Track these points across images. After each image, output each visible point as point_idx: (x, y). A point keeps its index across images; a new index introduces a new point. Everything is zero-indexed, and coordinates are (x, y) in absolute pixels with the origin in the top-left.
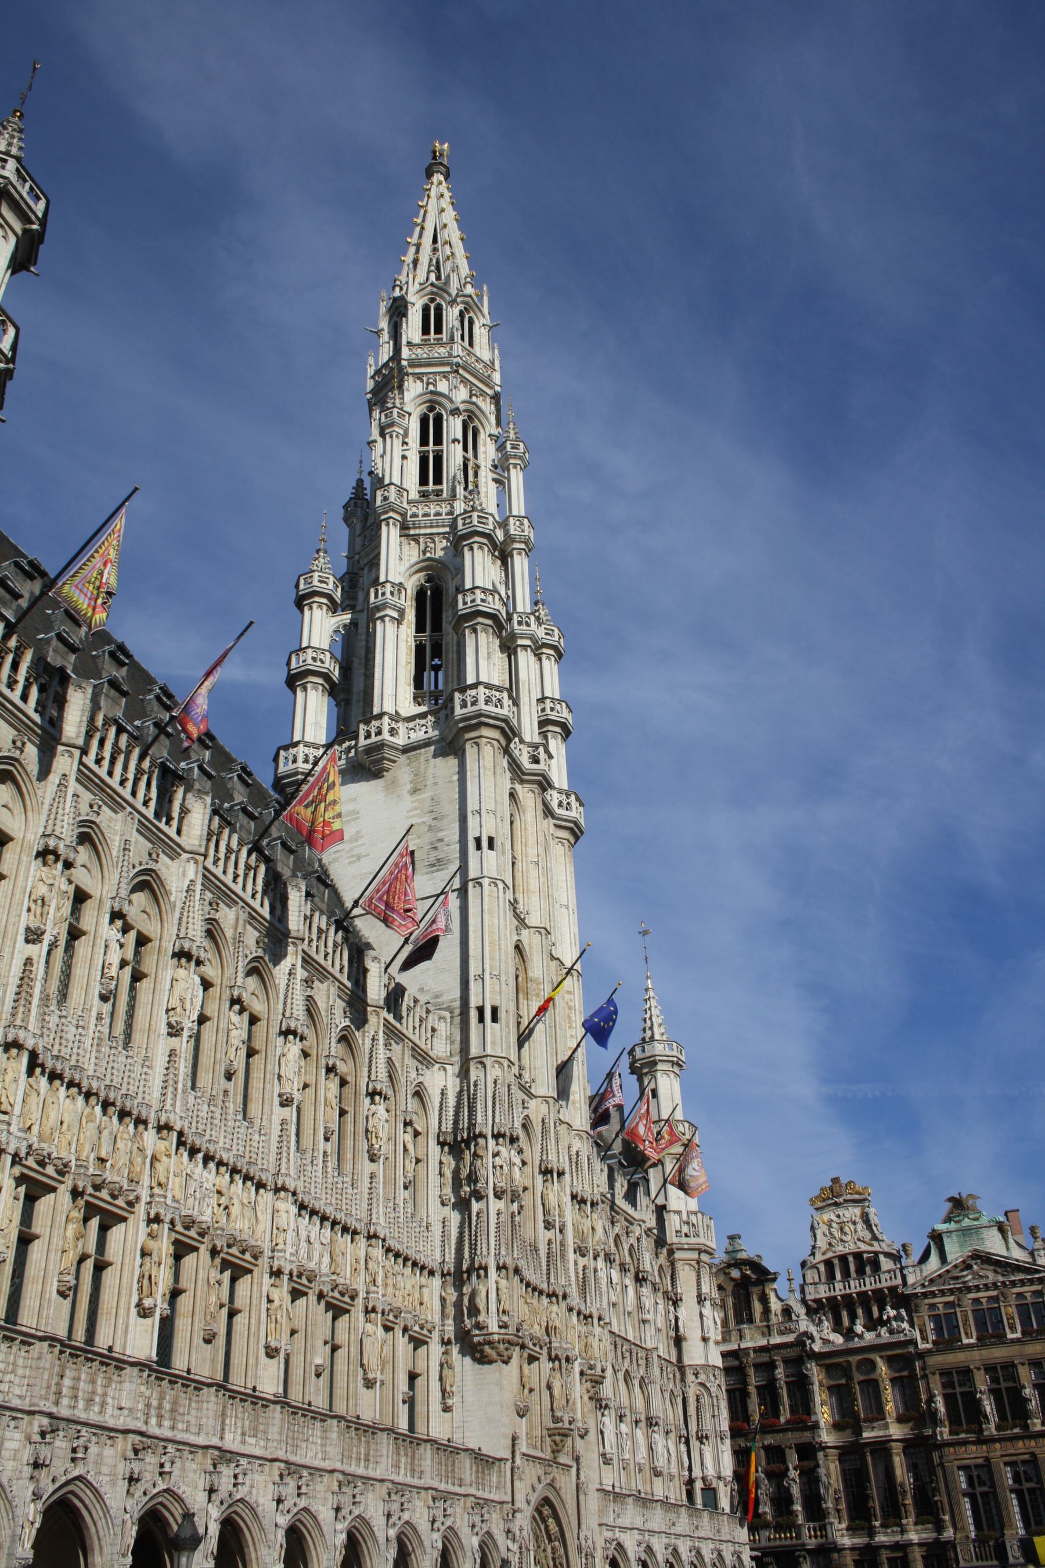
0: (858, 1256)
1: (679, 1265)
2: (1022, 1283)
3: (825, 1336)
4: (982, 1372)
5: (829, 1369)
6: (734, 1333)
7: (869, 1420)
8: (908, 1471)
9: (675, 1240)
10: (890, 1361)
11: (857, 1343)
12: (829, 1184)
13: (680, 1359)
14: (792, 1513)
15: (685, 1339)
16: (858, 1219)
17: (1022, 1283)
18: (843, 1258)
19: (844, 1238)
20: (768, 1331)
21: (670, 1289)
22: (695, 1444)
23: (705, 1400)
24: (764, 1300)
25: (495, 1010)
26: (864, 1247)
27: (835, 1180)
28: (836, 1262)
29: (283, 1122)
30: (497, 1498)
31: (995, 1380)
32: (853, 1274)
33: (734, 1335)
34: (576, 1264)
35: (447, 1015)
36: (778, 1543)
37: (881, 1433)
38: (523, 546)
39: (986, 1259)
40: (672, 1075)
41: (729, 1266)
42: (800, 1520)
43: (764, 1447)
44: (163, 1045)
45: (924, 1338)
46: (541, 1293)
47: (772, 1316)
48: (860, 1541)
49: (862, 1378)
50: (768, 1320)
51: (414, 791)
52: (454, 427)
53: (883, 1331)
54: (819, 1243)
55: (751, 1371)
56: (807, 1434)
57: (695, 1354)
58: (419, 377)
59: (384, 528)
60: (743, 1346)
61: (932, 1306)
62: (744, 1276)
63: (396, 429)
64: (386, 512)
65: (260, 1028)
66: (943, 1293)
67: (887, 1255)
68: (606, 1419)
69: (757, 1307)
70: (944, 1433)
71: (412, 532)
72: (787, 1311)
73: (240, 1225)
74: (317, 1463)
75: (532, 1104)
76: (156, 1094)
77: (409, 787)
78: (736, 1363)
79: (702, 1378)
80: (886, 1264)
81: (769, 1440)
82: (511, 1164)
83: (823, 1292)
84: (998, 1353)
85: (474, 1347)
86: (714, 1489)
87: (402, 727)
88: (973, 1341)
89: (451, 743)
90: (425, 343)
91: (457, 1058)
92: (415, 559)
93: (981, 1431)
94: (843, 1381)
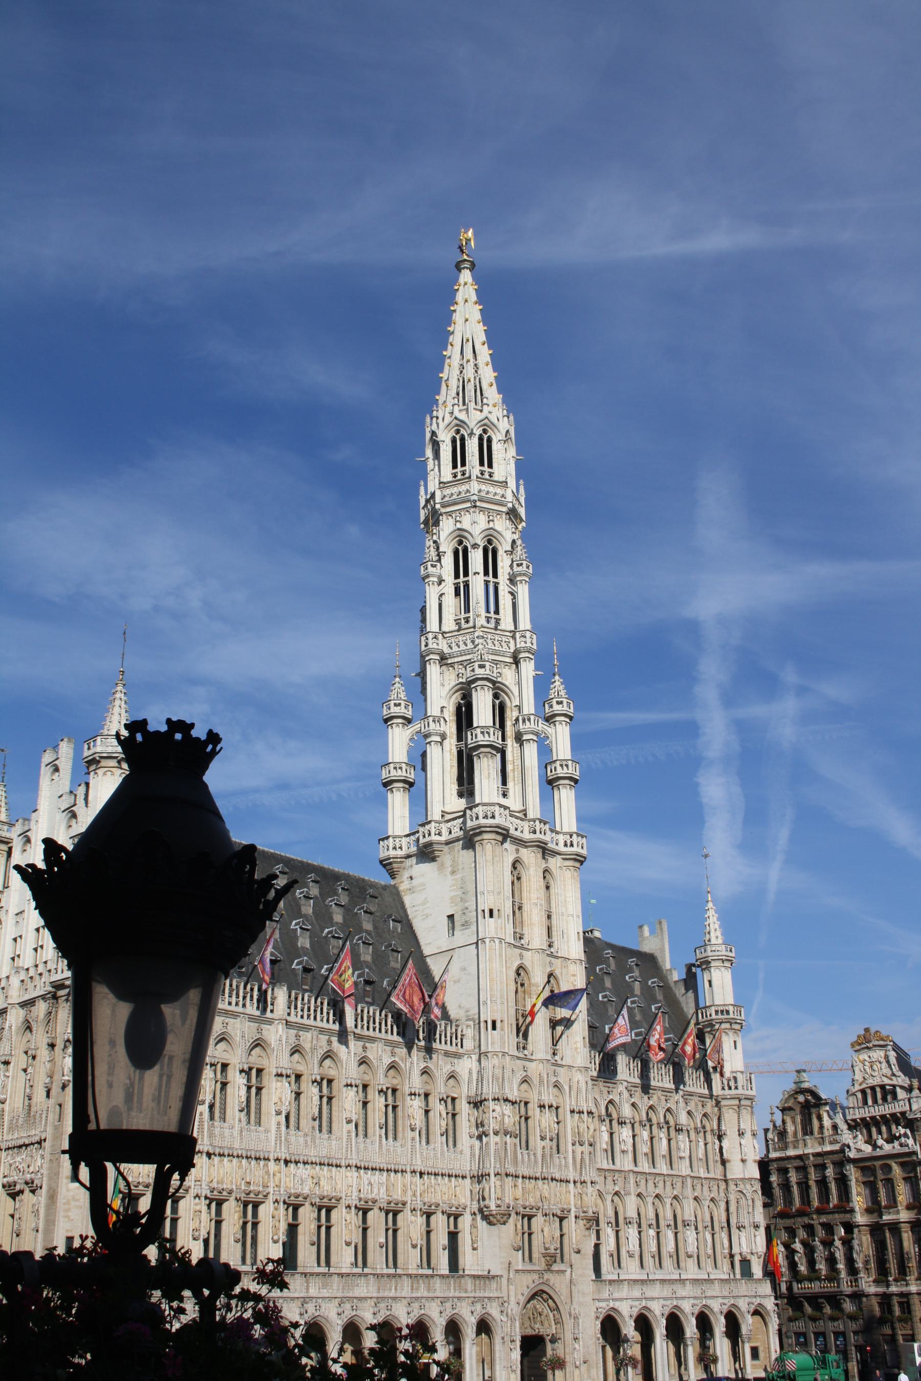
0: (882, 1087)
1: (723, 1110)
3: (858, 1146)
5: (863, 1169)
6: (801, 1142)
7: (887, 1207)
8: (914, 1243)
9: (721, 1092)
10: (902, 1165)
11: (879, 1153)
12: (863, 1032)
13: (725, 1176)
14: (837, 1271)
15: (729, 1161)
16: (882, 1060)
18: (873, 1088)
19: (874, 1074)
20: (822, 1141)
21: (715, 1127)
22: (734, 1230)
23: (743, 1202)
24: (820, 1118)
25: (494, 1023)
26: (886, 1081)
27: (867, 1030)
28: (869, 1091)
29: (349, 1132)
30: (496, 1295)
32: (880, 1101)
33: (801, 1143)
34: (573, 1152)
35: (471, 1023)
36: (826, 1290)
37: (894, 1217)
38: (527, 655)
40: (723, 969)
41: (797, 1093)
42: (843, 1275)
43: (820, 1224)
46: (536, 1179)
47: (825, 1131)
48: (881, 1290)
49: (883, 1177)
51: (453, 872)
52: (476, 559)
53: (896, 1143)
55: (812, 1170)
56: (848, 1216)
57: (736, 1171)
58: (449, 514)
59: (428, 666)
60: (806, 1152)
62: (807, 1101)
63: (431, 579)
64: (428, 655)
65: (335, 1084)
67: (902, 1087)
68: (630, 1231)
69: (816, 1123)
71: (450, 661)
72: (835, 1127)
73: (326, 1188)
74: (362, 1295)
75: (532, 1066)
76: (273, 1144)
77: (450, 869)
78: (801, 1164)
79: (741, 1187)
80: (901, 1094)
81: (824, 1219)
82: (504, 1115)
83: (858, 1114)
85: (485, 1218)
86: (749, 1261)
87: (444, 828)
89: (470, 840)
90: (455, 481)
91: (477, 1050)
92: (453, 683)
94: (872, 1179)
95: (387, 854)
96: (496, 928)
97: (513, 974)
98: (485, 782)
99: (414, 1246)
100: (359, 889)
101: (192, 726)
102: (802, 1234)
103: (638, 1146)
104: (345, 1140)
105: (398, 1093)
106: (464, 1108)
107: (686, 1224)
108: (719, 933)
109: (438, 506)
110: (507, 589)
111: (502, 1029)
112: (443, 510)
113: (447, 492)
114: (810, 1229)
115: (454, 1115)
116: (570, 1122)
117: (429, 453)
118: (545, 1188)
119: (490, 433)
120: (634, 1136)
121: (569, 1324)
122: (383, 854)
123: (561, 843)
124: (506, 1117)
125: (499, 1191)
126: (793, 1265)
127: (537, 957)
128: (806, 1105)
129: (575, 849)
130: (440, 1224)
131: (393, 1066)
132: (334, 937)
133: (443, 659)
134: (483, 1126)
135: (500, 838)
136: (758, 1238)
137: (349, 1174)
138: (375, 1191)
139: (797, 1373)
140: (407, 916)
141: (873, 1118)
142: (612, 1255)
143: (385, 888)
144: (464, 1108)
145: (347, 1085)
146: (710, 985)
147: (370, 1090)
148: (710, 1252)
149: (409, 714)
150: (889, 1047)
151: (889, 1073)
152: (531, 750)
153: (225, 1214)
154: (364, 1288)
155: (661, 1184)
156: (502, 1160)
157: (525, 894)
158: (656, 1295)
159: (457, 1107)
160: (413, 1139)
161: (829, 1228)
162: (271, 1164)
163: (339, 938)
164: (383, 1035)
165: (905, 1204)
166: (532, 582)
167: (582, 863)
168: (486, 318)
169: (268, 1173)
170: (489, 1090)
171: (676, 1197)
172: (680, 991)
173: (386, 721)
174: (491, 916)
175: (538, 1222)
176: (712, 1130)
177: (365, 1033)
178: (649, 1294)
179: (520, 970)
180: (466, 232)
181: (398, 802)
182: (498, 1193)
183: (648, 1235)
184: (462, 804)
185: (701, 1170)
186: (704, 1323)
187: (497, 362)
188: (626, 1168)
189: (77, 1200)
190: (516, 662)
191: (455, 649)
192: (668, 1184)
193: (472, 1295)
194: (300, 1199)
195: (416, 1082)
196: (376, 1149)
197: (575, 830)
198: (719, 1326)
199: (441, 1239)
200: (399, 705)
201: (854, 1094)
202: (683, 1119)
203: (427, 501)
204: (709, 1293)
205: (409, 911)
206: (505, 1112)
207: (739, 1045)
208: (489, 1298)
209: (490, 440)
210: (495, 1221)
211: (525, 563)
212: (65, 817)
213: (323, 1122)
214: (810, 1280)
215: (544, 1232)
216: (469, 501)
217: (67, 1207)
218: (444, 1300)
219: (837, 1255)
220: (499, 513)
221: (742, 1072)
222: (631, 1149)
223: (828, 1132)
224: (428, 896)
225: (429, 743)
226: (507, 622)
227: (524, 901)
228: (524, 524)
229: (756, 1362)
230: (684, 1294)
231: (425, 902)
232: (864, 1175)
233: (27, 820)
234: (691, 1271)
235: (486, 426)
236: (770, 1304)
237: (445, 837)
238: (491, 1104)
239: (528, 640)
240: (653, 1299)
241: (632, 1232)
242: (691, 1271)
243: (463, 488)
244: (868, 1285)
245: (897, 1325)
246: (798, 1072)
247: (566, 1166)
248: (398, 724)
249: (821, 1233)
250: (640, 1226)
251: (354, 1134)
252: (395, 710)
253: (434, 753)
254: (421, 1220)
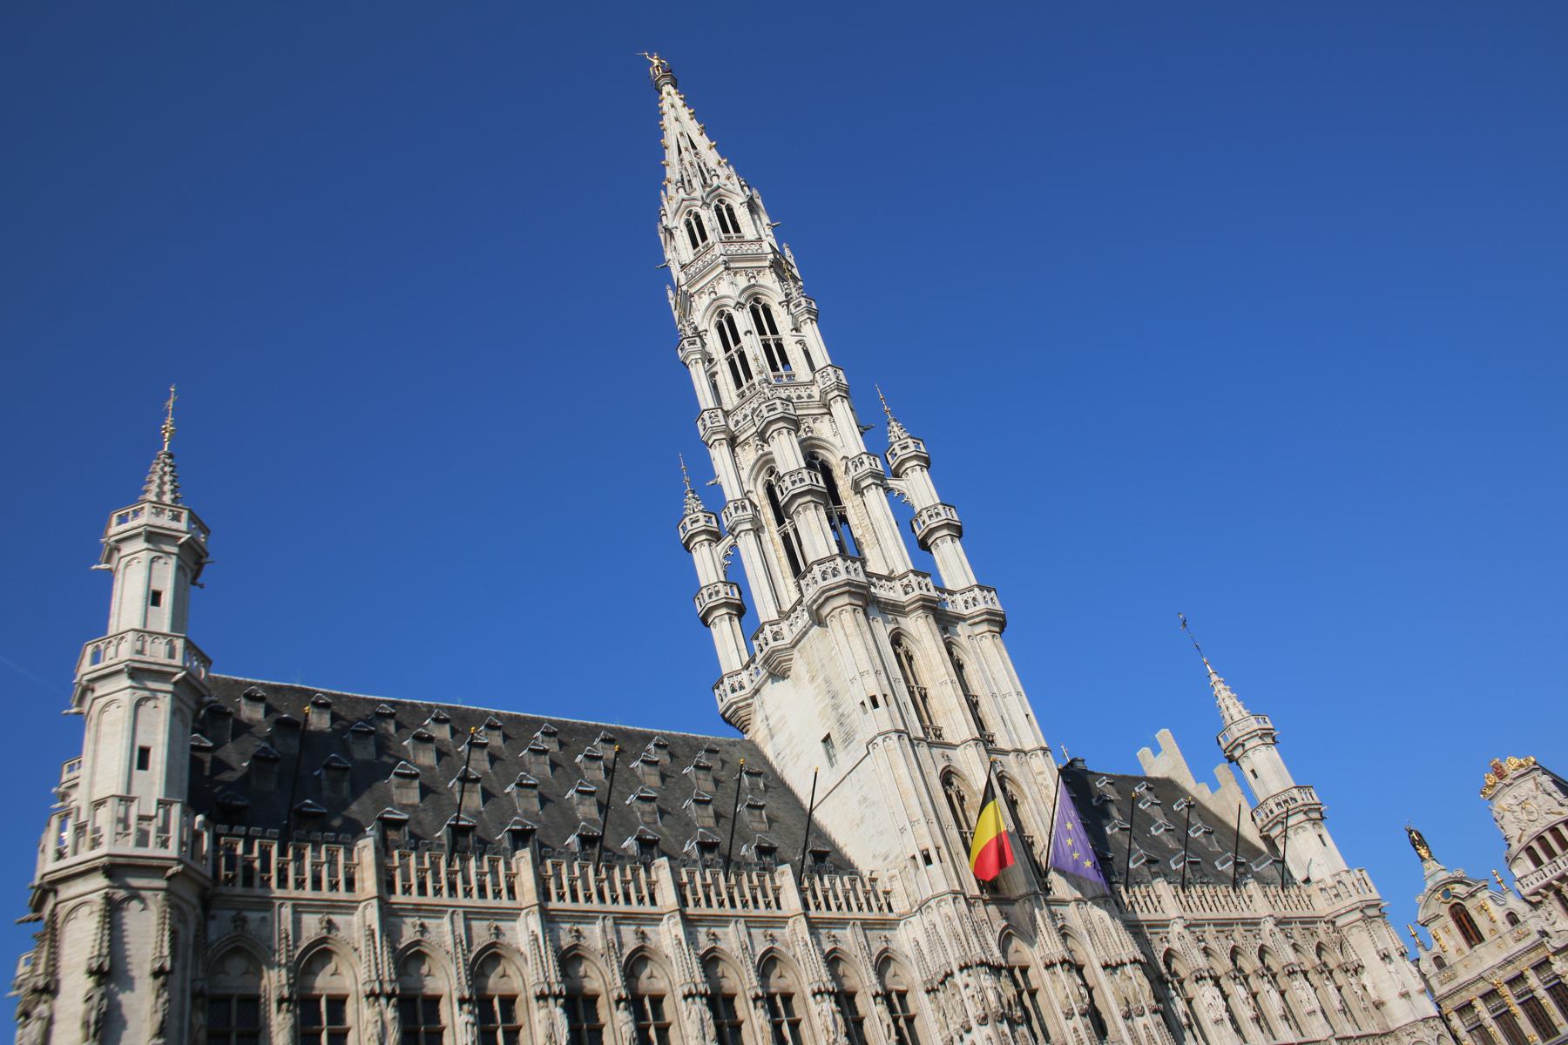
26: (1554, 819)
28: (1535, 845)
52: (744, 321)
69: (1481, 922)
71: (742, 438)
77: (807, 677)
87: (784, 625)
97: (936, 783)
112: (692, 290)
122: (721, 707)
143: (734, 744)
144: (919, 1002)
166: (817, 317)
167: (1002, 625)
177: (703, 909)
179: (947, 777)
190: (827, 406)
197: (974, 582)
205: (775, 764)
209: (730, 209)
238: (960, 979)
253: (747, 544)
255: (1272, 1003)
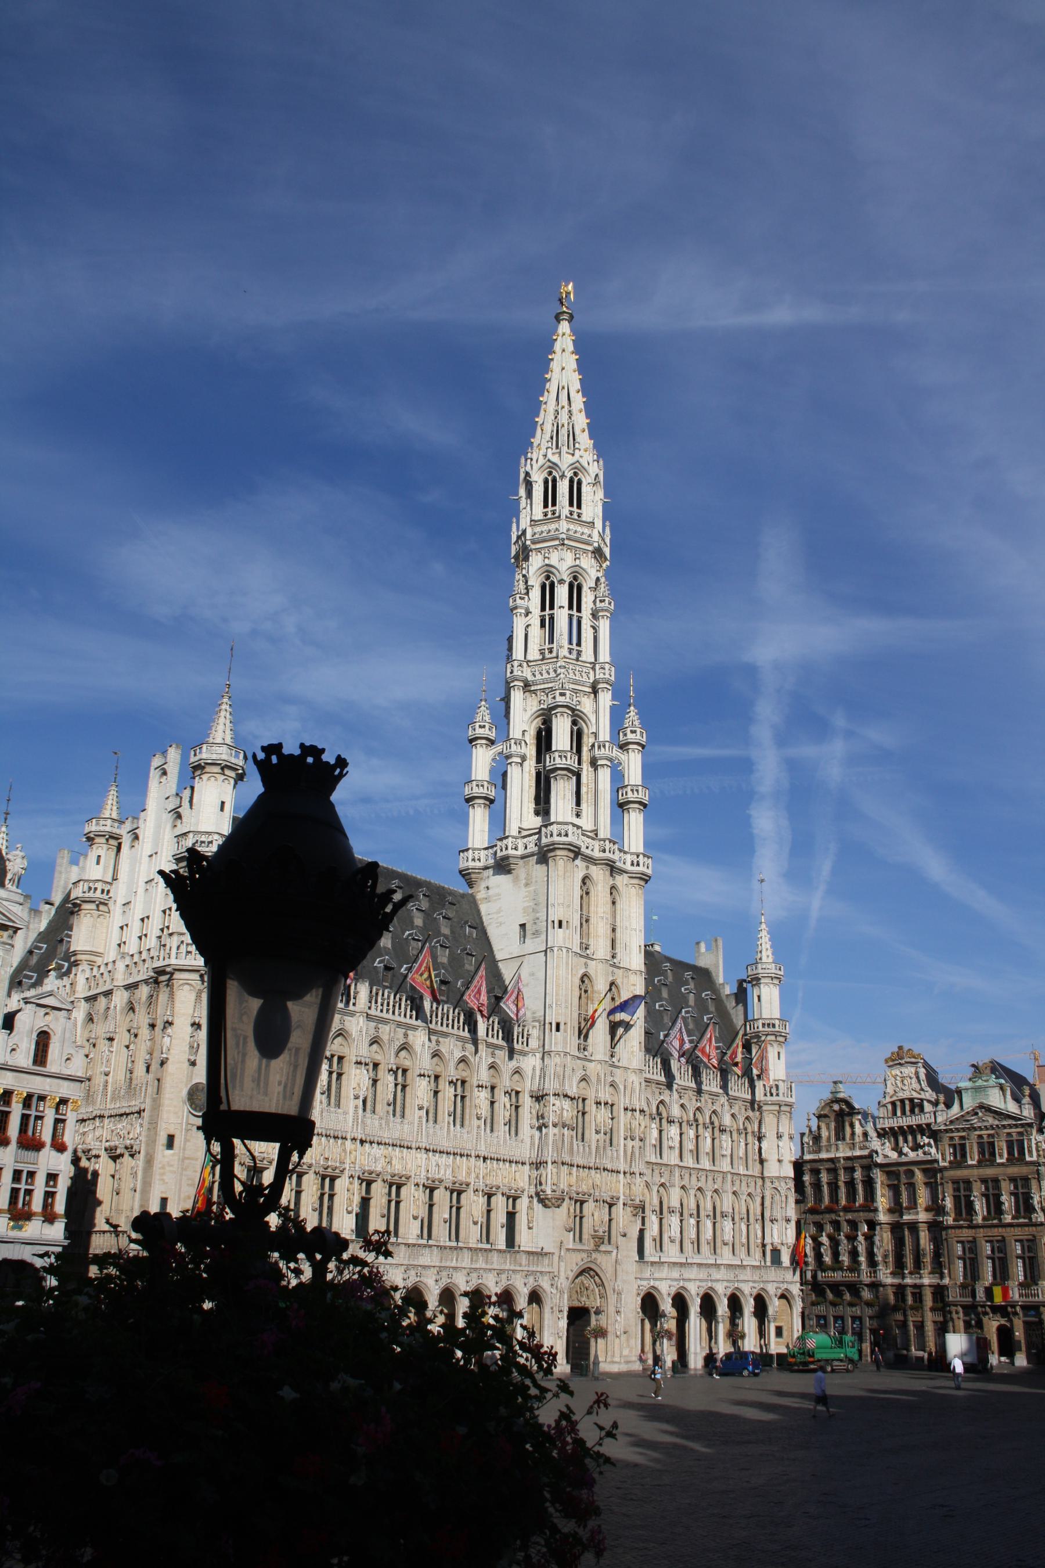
0: (911, 1100)
1: (764, 1114)
2: (1010, 1126)
3: (885, 1152)
4: (979, 1183)
5: (889, 1174)
6: (833, 1147)
7: (908, 1208)
8: (930, 1241)
9: (763, 1098)
10: (925, 1171)
11: (904, 1159)
12: (896, 1050)
14: (859, 1263)
16: (913, 1076)
17: (1010, 1126)
18: (902, 1101)
20: (853, 1146)
21: (756, 1129)
22: (767, 1223)
23: (777, 1198)
24: (852, 1126)
26: (915, 1095)
28: (898, 1103)
29: (420, 1117)
30: (547, 1270)
31: (987, 1188)
32: (908, 1113)
33: (833, 1148)
34: (625, 1145)
35: (537, 1024)
38: (605, 685)
39: (988, 1109)
41: (833, 1102)
42: (864, 1266)
44: (352, 1103)
45: (944, 1159)
46: (589, 1168)
48: (896, 1281)
50: (853, 1139)
51: (527, 885)
52: (562, 594)
53: (920, 1152)
54: (888, 1090)
55: (842, 1172)
56: (872, 1214)
57: (772, 1169)
58: (539, 550)
59: (512, 692)
60: (838, 1155)
61: (951, 1138)
62: (841, 1109)
63: (519, 610)
65: (409, 1073)
66: (958, 1130)
67: (929, 1101)
68: (673, 1219)
69: (848, 1130)
70: (950, 1220)
71: (532, 688)
72: (865, 1134)
73: (397, 1167)
75: (591, 1066)
79: (776, 1185)
81: (849, 1216)
82: (563, 1109)
83: (887, 1124)
84: (989, 1172)
85: (541, 1201)
87: (520, 843)
88: (974, 1163)
89: (544, 856)
90: (546, 519)
92: (535, 709)
93: (971, 1221)
95: (466, 864)
96: (564, 938)
97: (577, 981)
98: (560, 803)
99: (475, 1223)
100: (439, 896)
101: (323, 751)
102: (829, 1228)
103: (685, 1143)
104: (416, 1125)
105: (467, 1085)
106: (526, 1101)
107: (724, 1215)
108: (769, 953)
109: (528, 543)
110: (590, 623)
111: (565, 1031)
112: (533, 547)
113: (538, 529)
114: (837, 1225)
115: (517, 1107)
116: (623, 1119)
117: (522, 492)
118: (597, 1177)
119: (580, 476)
120: (681, 1134)
121: (612, 1298)
122: (462, 865)
123: (629, 863)
124: (565, 1113)
125: (555, 1177)
126: (818, 1256)
127: (600, 966)
128: (841, 1113)
129: (641, 869)
130: (500, 1204)
131: (463, 1060)
132: (414, 939)
133: (527, 686)
134: (543, 1118)
135: (572, 855)
136: (789, 1231)
137: (419, 1156)
138: (442, 1172)
139: (816, 1351)
140: (482, 923)
141: (901, 1128)
142: (655, 1240)
143: (463, 896)
144: (526, 1101)
145: (420, 1075)
146: (759, 1000)
147: (441, 1081)
148: (744, 1241)
149: (492, 735)
150: (920, 1065)
151: (918, 1088)
152: (605, 775)
153: (304, 1186)
154: (428, 1258)
155: (703, 1178)
156: (559, 1150)
157: (592, 909)
158: (692, 1277)
159: (521, 1100)
160: (479, 1127)
161: (854, 1225)
162: (348, 1143)
163: (418, 940)
164: (455, 1031)
165: (924, 1206)
166: (613, 618)
167: (646, 881)
168: (581, 367)
169: (344, 1151)
170: (551, 1086)
171: (716, 1191)
172: (730, 1004)
173: (471, 741)
174: (560, 926)
175: (589, 1207)
176: (753, 1132)
177: (439, 1028)
178: (686, 1276)
179: (585, 978)
180: (566, 285)
181: (479, 819)
182: (554, 1179)
183: (689, 1224)
184: (538, 821)
185: (741, 1168)
186: (735, 1303)
187: (590, 410)
188: (672, 1163)
189: (172, 1166)
190: (595, 691)
191: (538, 677)
192: (710, 1178)
193: (526, 1269)
194: (373, 1175)
195: (484, 1075)
196: (444, 1135)
197: (641, 850)
198: (749, 1307)
199: (499, 1218)
200: (484, 727)
201: (884, 1106)
202: (727, 1120)
203: (519, 537)
204: (742, 1277)
205: (484, 919)
206: (565, 1107)
207: (782, 1056)
208: (541, 1272)
209: (579, 483)
210: (550, 1204)
211: (607, 599)
212: (170, 817)
213: (397, 1107)
214: (833, 1270)
215: (594, 1215)
216: (557, 539)
217: (162, 1171)
218: (500, 1272)
219: (860, 1249)
220: (585, 551)
221: (783, 1081)
222: (678, 1145)
223: (859, 1138)
224: (502, 905)
225: (510, 763)
226: (588, 655)
227: (592, 915)
228: (608, 563)
229: (779, 1340)
230: (718, 1277)
231: (499, 911)
232: (889, 1179)
233: (136, 818)
234: (726, 1256)
235: (577, 469)
236: (796, 1289)
237: (520, 852)
238: (552, 1099)
239: (607, 672)
240: (690, 1280)
241: (675, 1220)
242: (726, 1256)
243: (553, 526)
244: (886, 1276)
245: (909, 1312)
246: (835, 1083)
247: (618, 1158)
248: (481, 745)
249: (846, 1228)
250: (682, 1215)
251: (424, 1120)
252: (479, 732)
253: (514, 772)
254: (482, 1200)
255: (706, 1145)
